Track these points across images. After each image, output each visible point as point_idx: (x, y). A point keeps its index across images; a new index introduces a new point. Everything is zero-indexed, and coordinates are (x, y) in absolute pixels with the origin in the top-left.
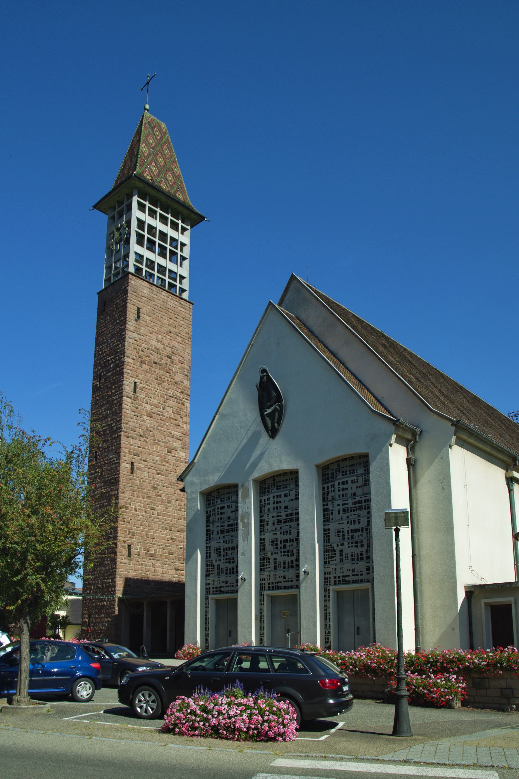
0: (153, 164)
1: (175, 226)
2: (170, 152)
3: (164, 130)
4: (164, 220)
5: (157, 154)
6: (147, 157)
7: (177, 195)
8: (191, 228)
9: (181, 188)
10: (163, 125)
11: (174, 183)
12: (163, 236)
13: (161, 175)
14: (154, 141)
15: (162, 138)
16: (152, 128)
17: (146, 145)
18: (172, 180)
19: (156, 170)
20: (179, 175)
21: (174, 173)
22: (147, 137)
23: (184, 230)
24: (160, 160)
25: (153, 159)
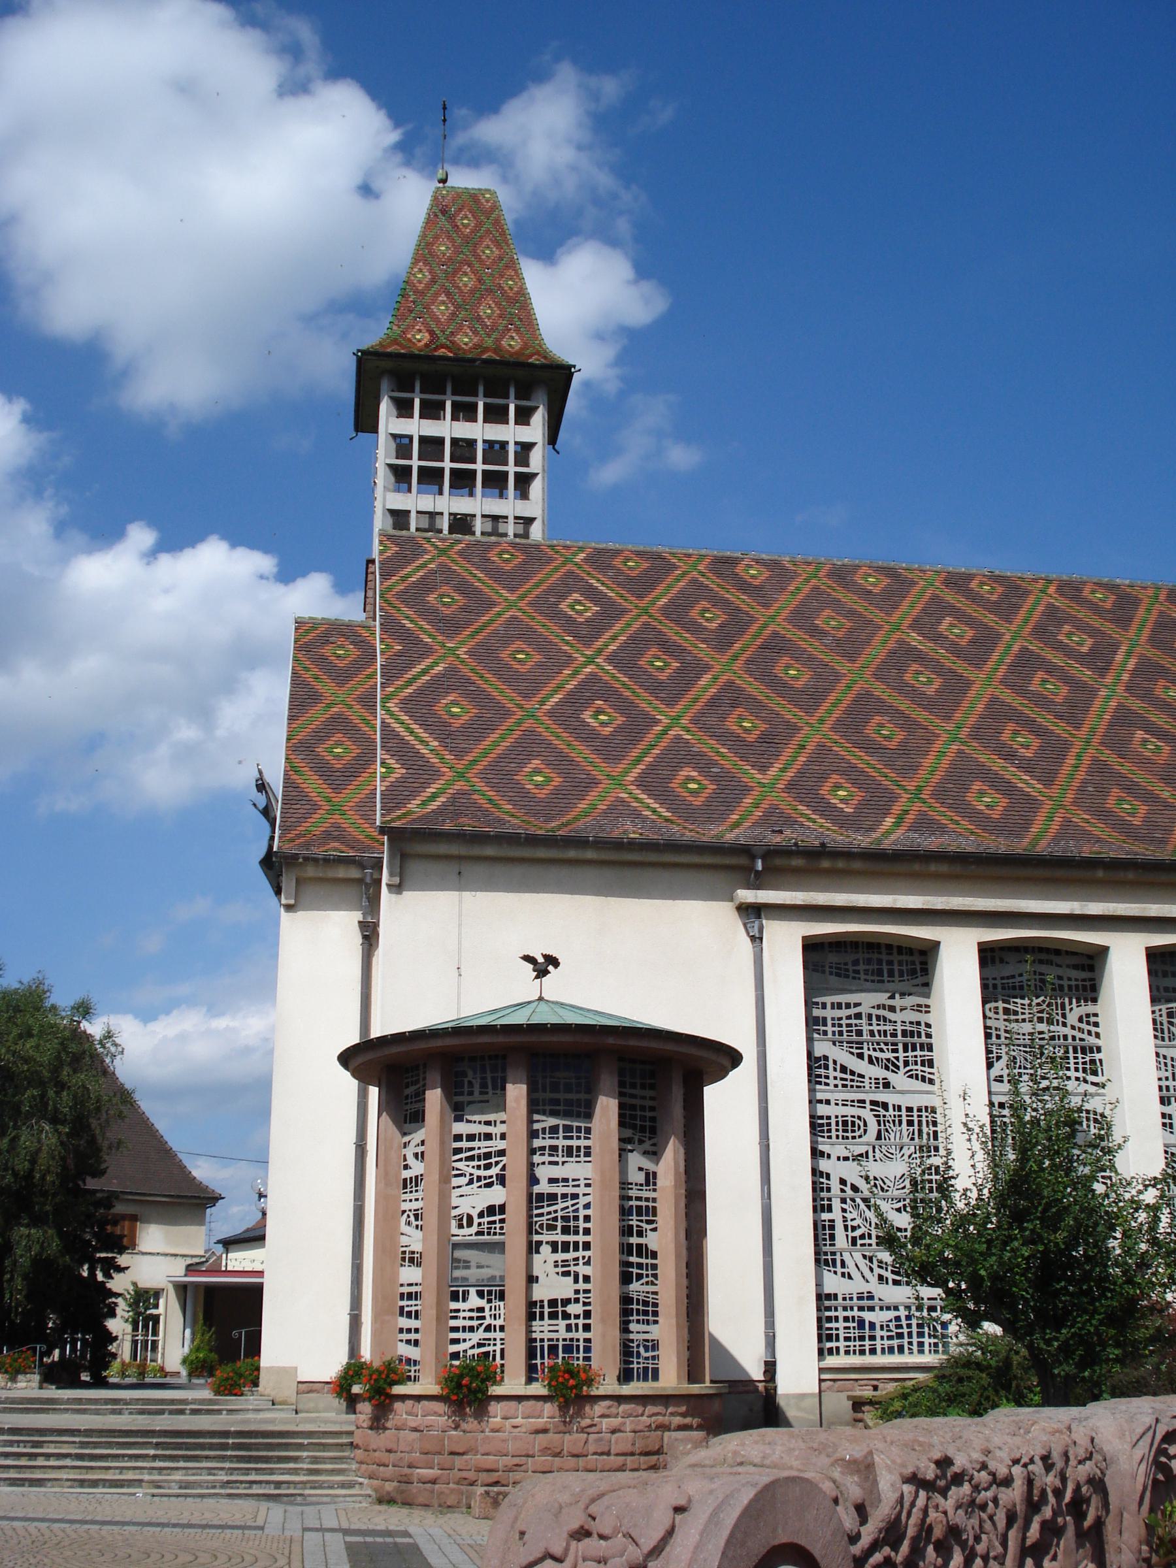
0: (443, 298)
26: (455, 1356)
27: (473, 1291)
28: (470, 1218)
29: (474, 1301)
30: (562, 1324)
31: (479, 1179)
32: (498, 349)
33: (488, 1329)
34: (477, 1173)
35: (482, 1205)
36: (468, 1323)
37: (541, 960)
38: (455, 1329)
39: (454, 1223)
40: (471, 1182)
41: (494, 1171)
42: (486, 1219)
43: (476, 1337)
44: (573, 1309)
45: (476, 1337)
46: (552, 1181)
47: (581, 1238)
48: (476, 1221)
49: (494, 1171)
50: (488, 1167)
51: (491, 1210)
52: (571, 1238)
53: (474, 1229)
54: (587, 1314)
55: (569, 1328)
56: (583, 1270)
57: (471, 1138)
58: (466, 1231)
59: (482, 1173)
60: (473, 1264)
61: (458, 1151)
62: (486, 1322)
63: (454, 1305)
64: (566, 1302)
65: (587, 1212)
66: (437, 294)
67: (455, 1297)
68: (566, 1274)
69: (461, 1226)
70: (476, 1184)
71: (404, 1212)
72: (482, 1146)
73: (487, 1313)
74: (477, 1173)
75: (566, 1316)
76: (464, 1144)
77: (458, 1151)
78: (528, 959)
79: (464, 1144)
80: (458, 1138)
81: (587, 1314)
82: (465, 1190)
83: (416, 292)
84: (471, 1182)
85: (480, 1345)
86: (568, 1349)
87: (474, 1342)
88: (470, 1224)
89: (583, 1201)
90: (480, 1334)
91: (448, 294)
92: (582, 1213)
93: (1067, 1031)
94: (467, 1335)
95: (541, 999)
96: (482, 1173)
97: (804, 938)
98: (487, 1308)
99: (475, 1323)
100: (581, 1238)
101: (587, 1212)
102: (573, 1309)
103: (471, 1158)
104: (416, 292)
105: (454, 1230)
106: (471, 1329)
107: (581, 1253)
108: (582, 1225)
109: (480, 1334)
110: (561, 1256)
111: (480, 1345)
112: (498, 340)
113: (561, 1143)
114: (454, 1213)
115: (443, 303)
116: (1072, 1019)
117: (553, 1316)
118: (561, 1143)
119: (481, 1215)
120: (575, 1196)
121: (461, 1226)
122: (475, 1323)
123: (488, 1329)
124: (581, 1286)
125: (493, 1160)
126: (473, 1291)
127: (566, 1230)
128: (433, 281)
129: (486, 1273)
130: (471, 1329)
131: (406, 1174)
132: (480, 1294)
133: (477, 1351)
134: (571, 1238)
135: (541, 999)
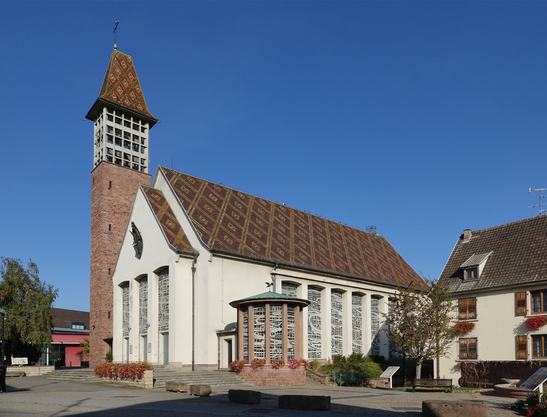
0: (119, 87)
1: (136, 127)
2: (134, 77)
3: (130, 61)
4: (127, 124)
5: (122, 80)
6: (114, 84)
7: (138, 107)
8: (150, 128)
9: (141, 101)
10: (130, 58)
11: (136, 98)
12: (127, 134)
13: (126, 94)
14: (121, 70)
15: (128, 67)
16: (120, 62)
17: (114, 74)
18: (134, 96)
19: (121, 91)
20: (140, 92)
21: (136, 91)
22: (114, 68)
23: (143, 130)
24: (125, 83)
25: (119, 83)
26: (271, 358)
27: (275, 347)
28: (274, 333)
29: (275, 348)
30: (290, 352)
31: (276, 326)
32: (136, 108)
33: (278, 353)
34: (275, 325)
35: (277, 331)
36: (274, 352)
37: (270, 284)
38: (272, 354)
39: (270, 334)
40: (274, 327)
41: (279, 325)
42: (277, 334)
43: (276, 355)
44: (292, 350)
45: (276, 355)
46: (289, 327)
47: (293, 337)
48: (275, 334)
49: (279, 325)
50: (277, 324)
51: (278, 332)
52: (291, 337)
53: (275, 335)
54: (294, 351)
55: (291, 353)
56: (293, 343)
57: (273, 318)
58: (273, 336)
59: (276, 325)
60: (275, 342)
61: (271, 321)
62: (278, 352)
63: (271, 349)
64: (291, 349)
65: (294, 333)
66: (118, 86)
67: (271, 348)
68: (291, 344)
69: (272, 335)
70: (275, 327)
71: (255, 332)
72: (277, 320)
73: (278, 351)
74: (275, 325)
75: (291, 351)
76: (272, 319)
77: (271, 321)
78: (267, 283)
79: (272, 319)
80: (271, 318)
81: (294, 351)
82: (273, 328)
83: (112, 83)
84: (274, 327)
85: (276, 356)
86: (291, 357)
87: (275, 356)
88: (274, 334)
89: (293, 331)
90: (277, 354)
91: (121, 87)
92: (293, 333)
93: (316, 302)
94: (274, 355)
95: (270, 291)
96: (276, 325)
97: (282, 281)
98: (278, 350)
99: (275, 352)
100: (293, 337)
101: (294, 333)
102: (292, 350)
103: (274, 322)
104: (112, 83)
105: (271, 336)
106: (275, 354)
107: (293, 340)
108: (293, 335)
109: (277, 354)
110: (290, 341)
111: (276, 356)
112: (136, 106)
113: (290, 320)
114: (270, 332)
115: (120, 89)
116: (317, 300)
117: (289, 351)
118: (290, 320)
119: (276, 333)
120: (292, 330)
121: (272, 335)
122: (275, 352)
123: (278, 353)
124: (293, 346)
125: (279, 323)
126: (275, 347)
127: (291, 336)
128: (116, 81)
129: (277, 344)
130: (275, 354)
131: (256, 324)
132: (276, 347)
133: (276, 357)
134: (291, 337)
135: (270, 291)
